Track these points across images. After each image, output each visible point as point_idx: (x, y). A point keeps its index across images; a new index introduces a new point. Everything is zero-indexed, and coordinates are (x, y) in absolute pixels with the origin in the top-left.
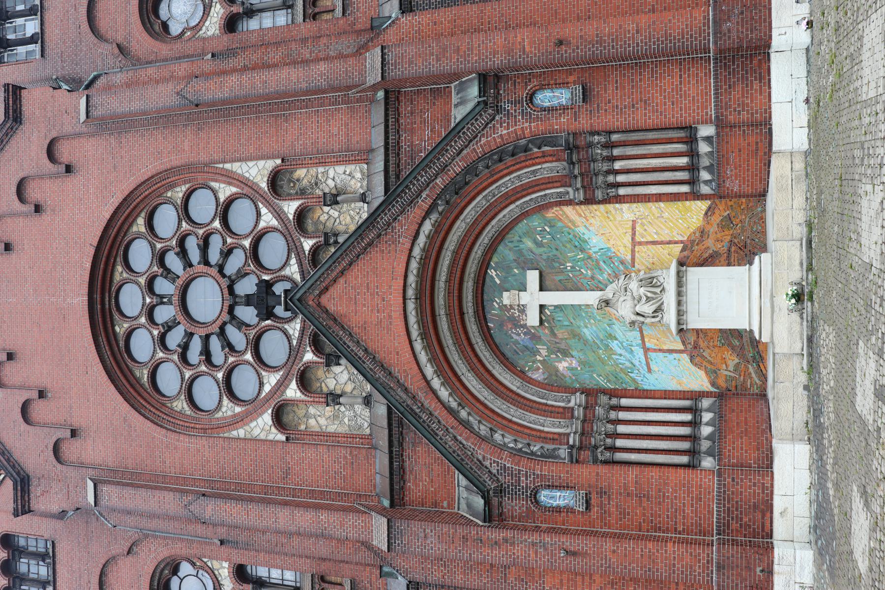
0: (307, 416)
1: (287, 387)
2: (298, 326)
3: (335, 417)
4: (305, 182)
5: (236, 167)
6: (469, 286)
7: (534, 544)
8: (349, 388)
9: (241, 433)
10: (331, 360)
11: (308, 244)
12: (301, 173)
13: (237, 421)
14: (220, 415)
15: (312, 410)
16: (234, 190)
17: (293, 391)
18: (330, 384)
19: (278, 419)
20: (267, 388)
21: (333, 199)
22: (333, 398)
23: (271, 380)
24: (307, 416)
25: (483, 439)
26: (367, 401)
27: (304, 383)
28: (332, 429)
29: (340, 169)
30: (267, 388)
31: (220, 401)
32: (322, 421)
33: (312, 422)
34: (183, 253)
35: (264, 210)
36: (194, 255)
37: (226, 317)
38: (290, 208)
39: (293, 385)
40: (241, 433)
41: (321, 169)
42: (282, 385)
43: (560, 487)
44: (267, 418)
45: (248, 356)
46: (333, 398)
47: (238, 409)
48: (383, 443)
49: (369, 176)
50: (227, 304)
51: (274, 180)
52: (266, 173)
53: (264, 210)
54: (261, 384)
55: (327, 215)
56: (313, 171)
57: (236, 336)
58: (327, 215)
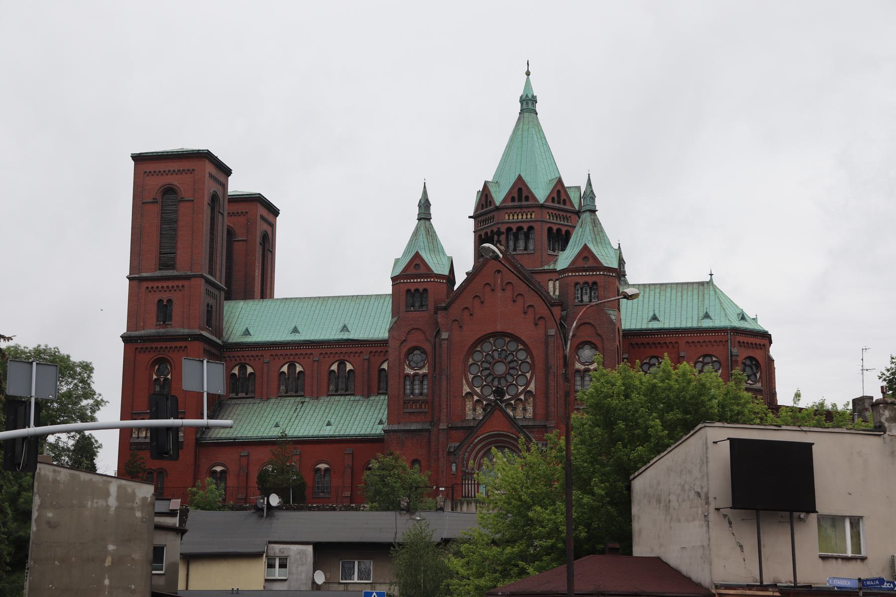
0: (470, 401)
1: (477, 396)
2: (492, 398)
3: (470, 410)
4: (529, 400)
5: (534, 380)
6: (502, 444)
7: (444, 463)
8: (477, 413)
9: (464, 382)
10: (484, 410)
11: (513, 402)
12: (532, 399)
13: (467, 380)
14: (469, 374)
15: (471, 403)
16: (529, 378)
17: (476, 398)
18: (478, 408)
19: (468, 393)
20: (476, 389)
21: (525, 409)
22: (474, 410)
23: (478, 390)
24: (470, 401)
25: (466, 450)
26: (474, 419)
27: (478, 401)
28: (467, 409)
29: (532, 410)
30: (476, 389)
31: (473, 374)
32: (468, 406)
33: (468, 403)
34: (512, 361)
35: (523, 388)
36: (512, 365)
37: (495, 376)
38: (522, 397)
39: (477, 398)
40: (464, 382)
41: (532, 405)
42: (477, 394)
43: (456, 468)
44: (469, 390)
45: (484, 383)
46: (474, 410)
47: (470, 380)
48: (464, 425)
49: (529, 419)
50: (498, 376)
51: (530, 392)
52: (531, 390)
53: (523, 388)
54: (477, 387)
55: (520, 407)
56: (532, 403)
57: (490, 379)
58: (520, 407)
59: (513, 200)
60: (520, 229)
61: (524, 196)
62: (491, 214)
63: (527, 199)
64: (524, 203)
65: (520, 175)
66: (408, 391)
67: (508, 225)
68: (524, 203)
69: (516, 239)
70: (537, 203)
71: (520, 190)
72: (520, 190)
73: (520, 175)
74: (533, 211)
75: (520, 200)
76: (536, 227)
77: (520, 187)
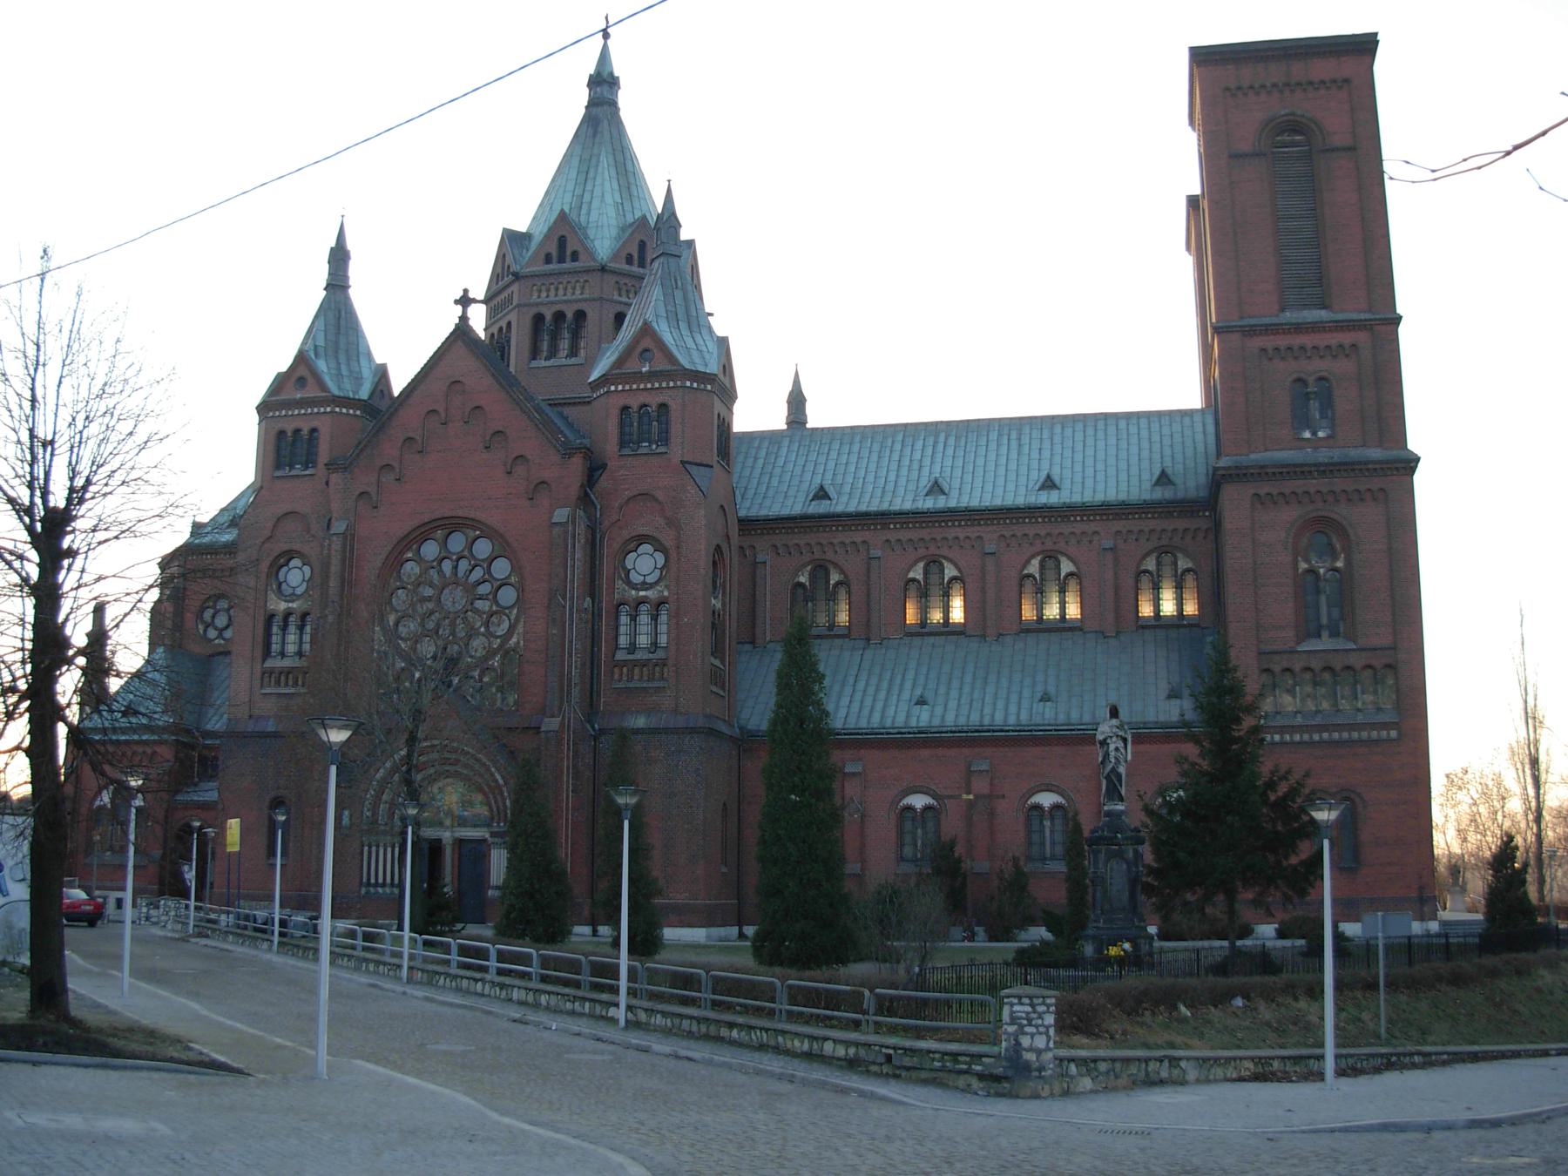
59: (548, 259)
60: (559, 316)
61: (568, 253)
62: (509, 291)
63: (575, 256)
64: (567, 265)
65: (562, 211)
66: (275, 647)
67: (534, 311)
68: (567, 265)
69: (555, 338)
70: (592, 263)
71: (562, 242)
72: (562, 242)
73: (562, 211)
74: (586, 281)
75: (561, 260)
76: (590, 315)
77: (564, 233)
